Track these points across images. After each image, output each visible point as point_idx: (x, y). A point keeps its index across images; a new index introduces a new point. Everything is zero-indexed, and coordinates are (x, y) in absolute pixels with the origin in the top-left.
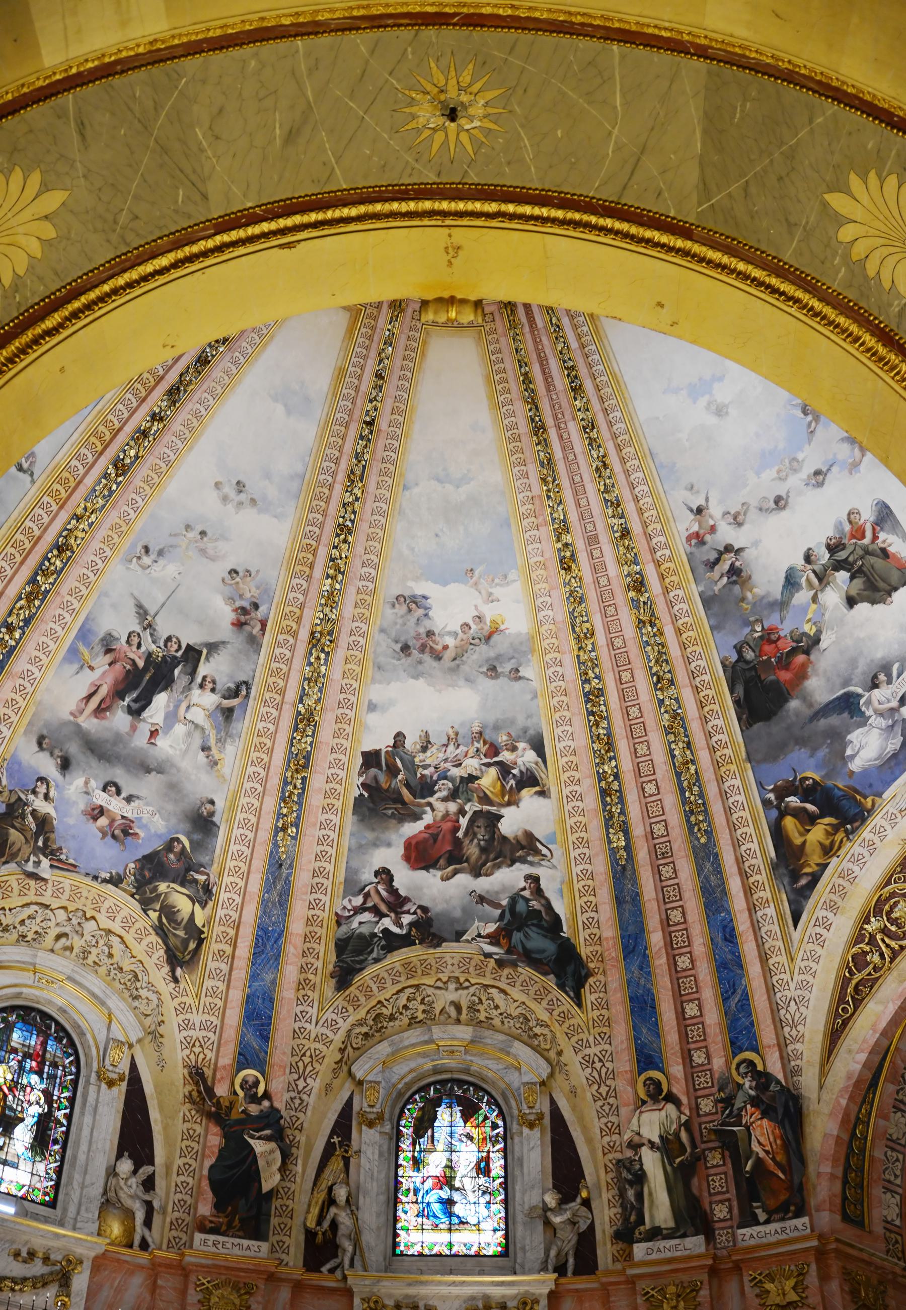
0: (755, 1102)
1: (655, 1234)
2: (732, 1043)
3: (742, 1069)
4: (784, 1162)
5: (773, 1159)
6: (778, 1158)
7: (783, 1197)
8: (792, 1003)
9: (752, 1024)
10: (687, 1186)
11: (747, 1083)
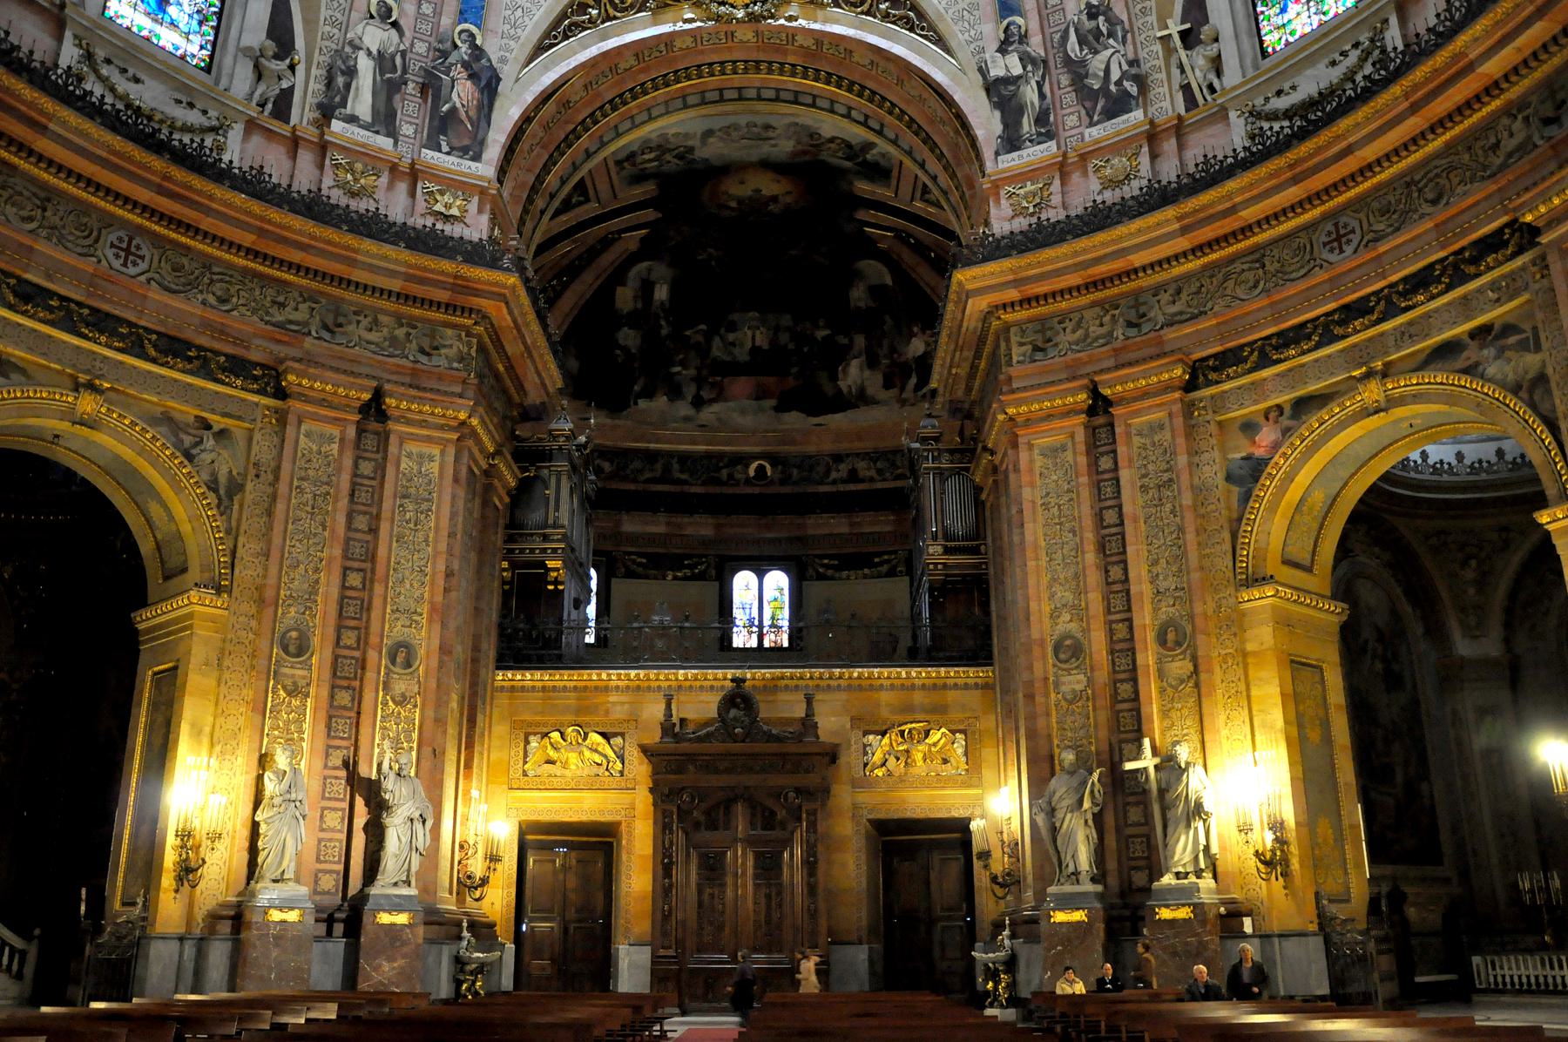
0: (466, 65)
1: (352, 119)
2: (461, 13)
3: (464, 36)
4: (475, 118)
5: (466, 112)
6: (471, 113)
7: (466, 142)
8: (520, 10)
9: (483, 8)
10: (389, 99)
11: (464, 48)
